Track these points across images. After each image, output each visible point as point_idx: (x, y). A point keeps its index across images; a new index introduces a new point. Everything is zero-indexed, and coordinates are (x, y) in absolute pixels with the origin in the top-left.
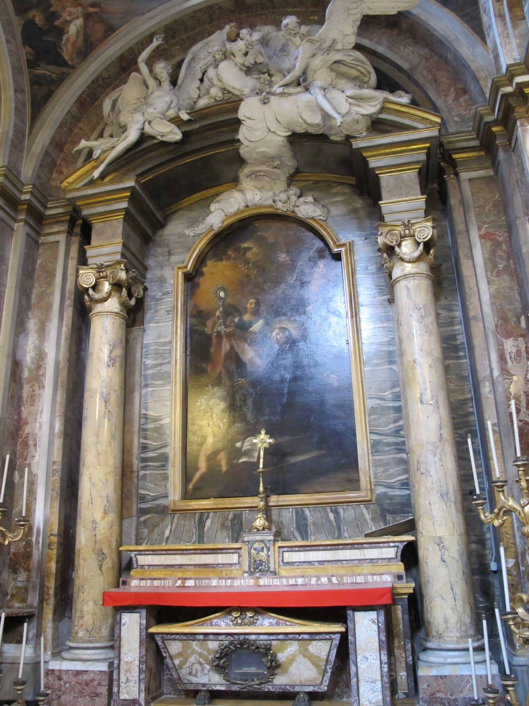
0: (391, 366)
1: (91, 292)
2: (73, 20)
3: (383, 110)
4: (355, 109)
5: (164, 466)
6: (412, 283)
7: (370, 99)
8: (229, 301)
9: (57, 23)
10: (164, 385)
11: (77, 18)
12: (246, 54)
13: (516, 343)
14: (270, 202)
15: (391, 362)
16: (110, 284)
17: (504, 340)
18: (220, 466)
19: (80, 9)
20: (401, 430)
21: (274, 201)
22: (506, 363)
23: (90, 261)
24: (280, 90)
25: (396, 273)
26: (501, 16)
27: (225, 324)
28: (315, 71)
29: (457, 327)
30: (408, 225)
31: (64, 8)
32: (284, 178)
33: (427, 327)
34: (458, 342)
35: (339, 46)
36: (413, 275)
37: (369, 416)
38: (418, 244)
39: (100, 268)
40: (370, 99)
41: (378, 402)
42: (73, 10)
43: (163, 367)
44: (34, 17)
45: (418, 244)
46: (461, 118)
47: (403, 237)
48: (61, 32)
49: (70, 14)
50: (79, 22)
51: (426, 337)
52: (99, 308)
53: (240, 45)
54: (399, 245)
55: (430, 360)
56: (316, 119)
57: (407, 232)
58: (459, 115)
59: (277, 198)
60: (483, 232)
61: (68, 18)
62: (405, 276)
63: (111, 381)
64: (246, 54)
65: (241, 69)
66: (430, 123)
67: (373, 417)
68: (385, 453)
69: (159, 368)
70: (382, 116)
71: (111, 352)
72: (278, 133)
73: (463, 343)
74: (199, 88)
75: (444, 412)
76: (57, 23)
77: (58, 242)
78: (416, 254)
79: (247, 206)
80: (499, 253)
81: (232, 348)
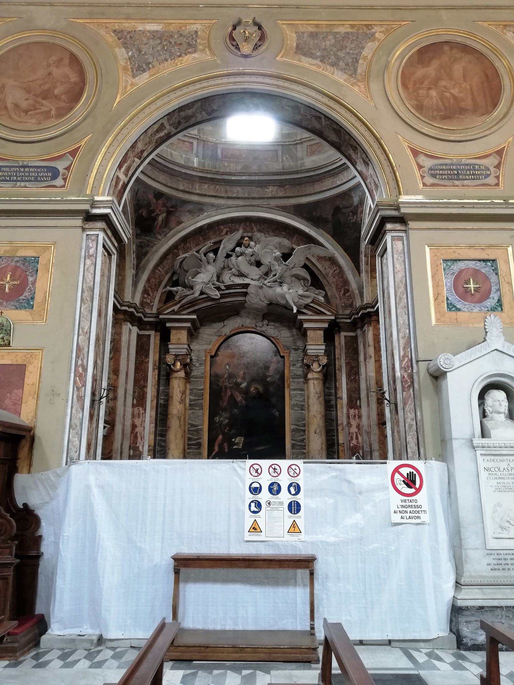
0: (302, 412)
1: (172, 366)
2: (161, 213)
3: (312, 302)
4: (300, 301)
5: (199, 448)
6: (316, 382)
7: (308, 297)
8: (230, 371)
9: (153, 215)
10: (200, 410)
11: (163, 213)
12: (252, 256)
13: (354, 411)
14: (253, 325)
15: (302, 410)
16: (181, 364)
17: (350, 410)
18: (225, 449)
19: (165, 209)
20: (305, 440)
21: (256, 326)
22: (350, 419)
23: (170, 350)
24: (269, 284)
25: (310, 376)
26: (367, 272)
27: (228, 382)
28: (285, 278)
29: (332, 397)
30: (317, 356)
31: (157, 208)
32: (261, 315)
33: (320, 402)
34: (332, 404)
35: (297, 266)
36: (317, 379)
37: (292, 432)
38: (321, 365)
39: (176, 356)
40: (308, 297)
41: (296, 427)
42: (162, 209)
43: (199, 401)
44: (143, 212)
45: (320, 365)
46: (345, 304)
47: (314, 361)
48: (155, 219)
49: (160, 211)
50: (164, 215)
51: (319, 406)
52: (176, 375)
53: (249, 251)
54: (312, 365)
55: (320, 416)
56: (283, 302)
57: (316, 359)
58: (344, 303)
59: (257, 324)
60: (347, 361)
61: (159, 213)
62: (313, 379)
63: (181, 410)
64: (252, 256)
65: (248, 263)
66: (331, 313)
67: (293, 433)
68: (297, 449)
69: (197, 401)
70: (312, 305)
71: (181, 397)
72: (265, 302)
73: (333, 405)
74: (224, 262)
75: (324, 437)
76: (153, 215)
77: (149, 336)
78: (319, 370)
79: (243, 326)
80: (353, 371)
81: (232, 395)
